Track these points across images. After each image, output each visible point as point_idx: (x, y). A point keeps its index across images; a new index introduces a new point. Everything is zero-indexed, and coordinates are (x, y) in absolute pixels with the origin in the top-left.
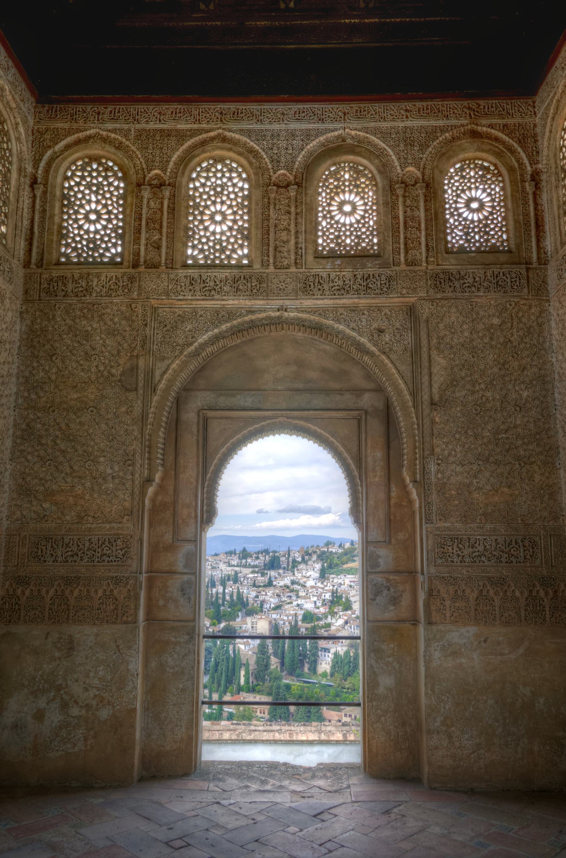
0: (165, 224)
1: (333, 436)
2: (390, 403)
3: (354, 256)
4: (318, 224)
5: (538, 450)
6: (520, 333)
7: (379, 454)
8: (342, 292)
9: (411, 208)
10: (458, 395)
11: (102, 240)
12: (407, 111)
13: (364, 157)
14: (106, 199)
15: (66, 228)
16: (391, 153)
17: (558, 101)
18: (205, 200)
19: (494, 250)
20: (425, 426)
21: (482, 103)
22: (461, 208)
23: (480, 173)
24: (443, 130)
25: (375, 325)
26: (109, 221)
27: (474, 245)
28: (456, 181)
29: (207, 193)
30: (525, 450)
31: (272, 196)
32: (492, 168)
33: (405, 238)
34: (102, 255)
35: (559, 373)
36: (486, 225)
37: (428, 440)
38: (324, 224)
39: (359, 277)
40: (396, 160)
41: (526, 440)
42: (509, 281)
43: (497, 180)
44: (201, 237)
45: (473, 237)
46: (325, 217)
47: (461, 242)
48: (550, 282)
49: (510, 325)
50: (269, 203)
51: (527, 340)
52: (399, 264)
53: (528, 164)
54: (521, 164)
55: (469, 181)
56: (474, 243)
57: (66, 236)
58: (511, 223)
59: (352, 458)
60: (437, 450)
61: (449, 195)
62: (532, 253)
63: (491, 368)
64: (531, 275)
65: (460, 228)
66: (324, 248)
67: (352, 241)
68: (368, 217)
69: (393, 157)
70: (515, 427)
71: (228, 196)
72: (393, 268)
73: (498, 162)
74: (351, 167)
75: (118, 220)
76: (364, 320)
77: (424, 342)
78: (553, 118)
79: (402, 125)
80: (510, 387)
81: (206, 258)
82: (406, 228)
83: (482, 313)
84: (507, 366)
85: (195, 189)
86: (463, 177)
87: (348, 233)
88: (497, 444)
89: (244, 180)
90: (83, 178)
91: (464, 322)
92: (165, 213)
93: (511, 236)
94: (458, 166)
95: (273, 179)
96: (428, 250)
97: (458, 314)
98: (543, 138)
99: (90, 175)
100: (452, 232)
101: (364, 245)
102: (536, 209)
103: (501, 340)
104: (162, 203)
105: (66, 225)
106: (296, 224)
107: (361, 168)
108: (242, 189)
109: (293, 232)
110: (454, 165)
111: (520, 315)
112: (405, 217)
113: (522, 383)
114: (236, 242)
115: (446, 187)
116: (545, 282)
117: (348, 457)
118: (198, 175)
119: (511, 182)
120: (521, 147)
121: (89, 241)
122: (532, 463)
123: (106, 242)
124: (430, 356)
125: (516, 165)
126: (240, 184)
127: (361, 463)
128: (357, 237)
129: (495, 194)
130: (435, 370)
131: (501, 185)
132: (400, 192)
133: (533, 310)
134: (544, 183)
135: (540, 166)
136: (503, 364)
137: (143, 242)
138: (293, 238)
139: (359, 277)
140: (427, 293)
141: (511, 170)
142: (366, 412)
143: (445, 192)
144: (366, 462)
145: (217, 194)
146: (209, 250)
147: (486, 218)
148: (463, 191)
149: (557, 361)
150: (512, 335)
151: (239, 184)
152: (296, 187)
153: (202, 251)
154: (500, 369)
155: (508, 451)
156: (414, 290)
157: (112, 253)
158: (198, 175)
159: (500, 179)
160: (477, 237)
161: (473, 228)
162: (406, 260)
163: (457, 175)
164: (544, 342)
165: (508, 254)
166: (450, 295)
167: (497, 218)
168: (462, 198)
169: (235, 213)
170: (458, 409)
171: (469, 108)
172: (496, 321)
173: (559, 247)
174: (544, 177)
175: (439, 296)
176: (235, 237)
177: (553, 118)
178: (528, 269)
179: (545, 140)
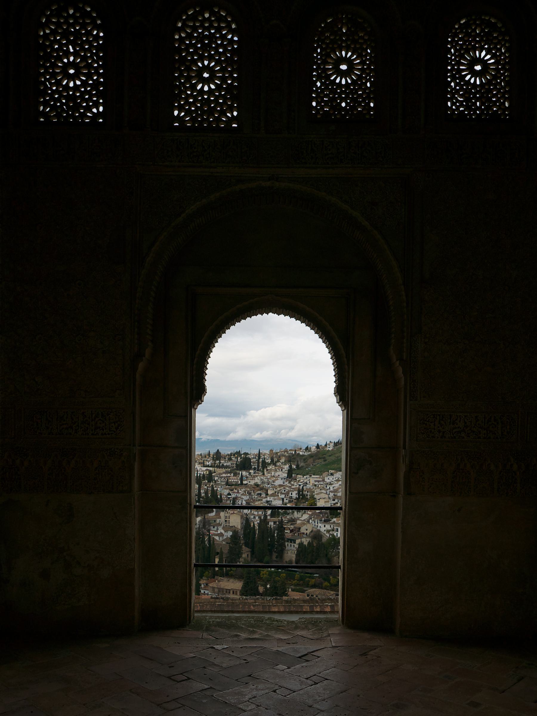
11: (82, 97)
14: (85, 50)
15: (44, 83)
18: (192, 54)
22: (463, 70)
26: (89, 76)
28: (460, 39)
29: (194, 46)
32: (499, 25)
34: (83, 115)
38: (319, 84)
43: (503, 39)
44: (188, 97)
46: (319, 78)
57: (44, 93)
61: (452, 55)
66: (318, 111)
68: (366, 77)
71: (216, 49)
75: (99, 75)
81: (193, 120)
86: (468, 35)
90: (58, 25)
99: (66, 22)
105: (43, 79)
114: (225, 102)
121: (68, 98)
123: (87, 101)
129: (500, 56)
145: (205, 47)
146: (196, 111)
153: (188, 112)
157: (93, 113)
163: (461, 32)
167: (500, 83)
168: (465, 59)
169: (222, 70)
176: (224, 97)
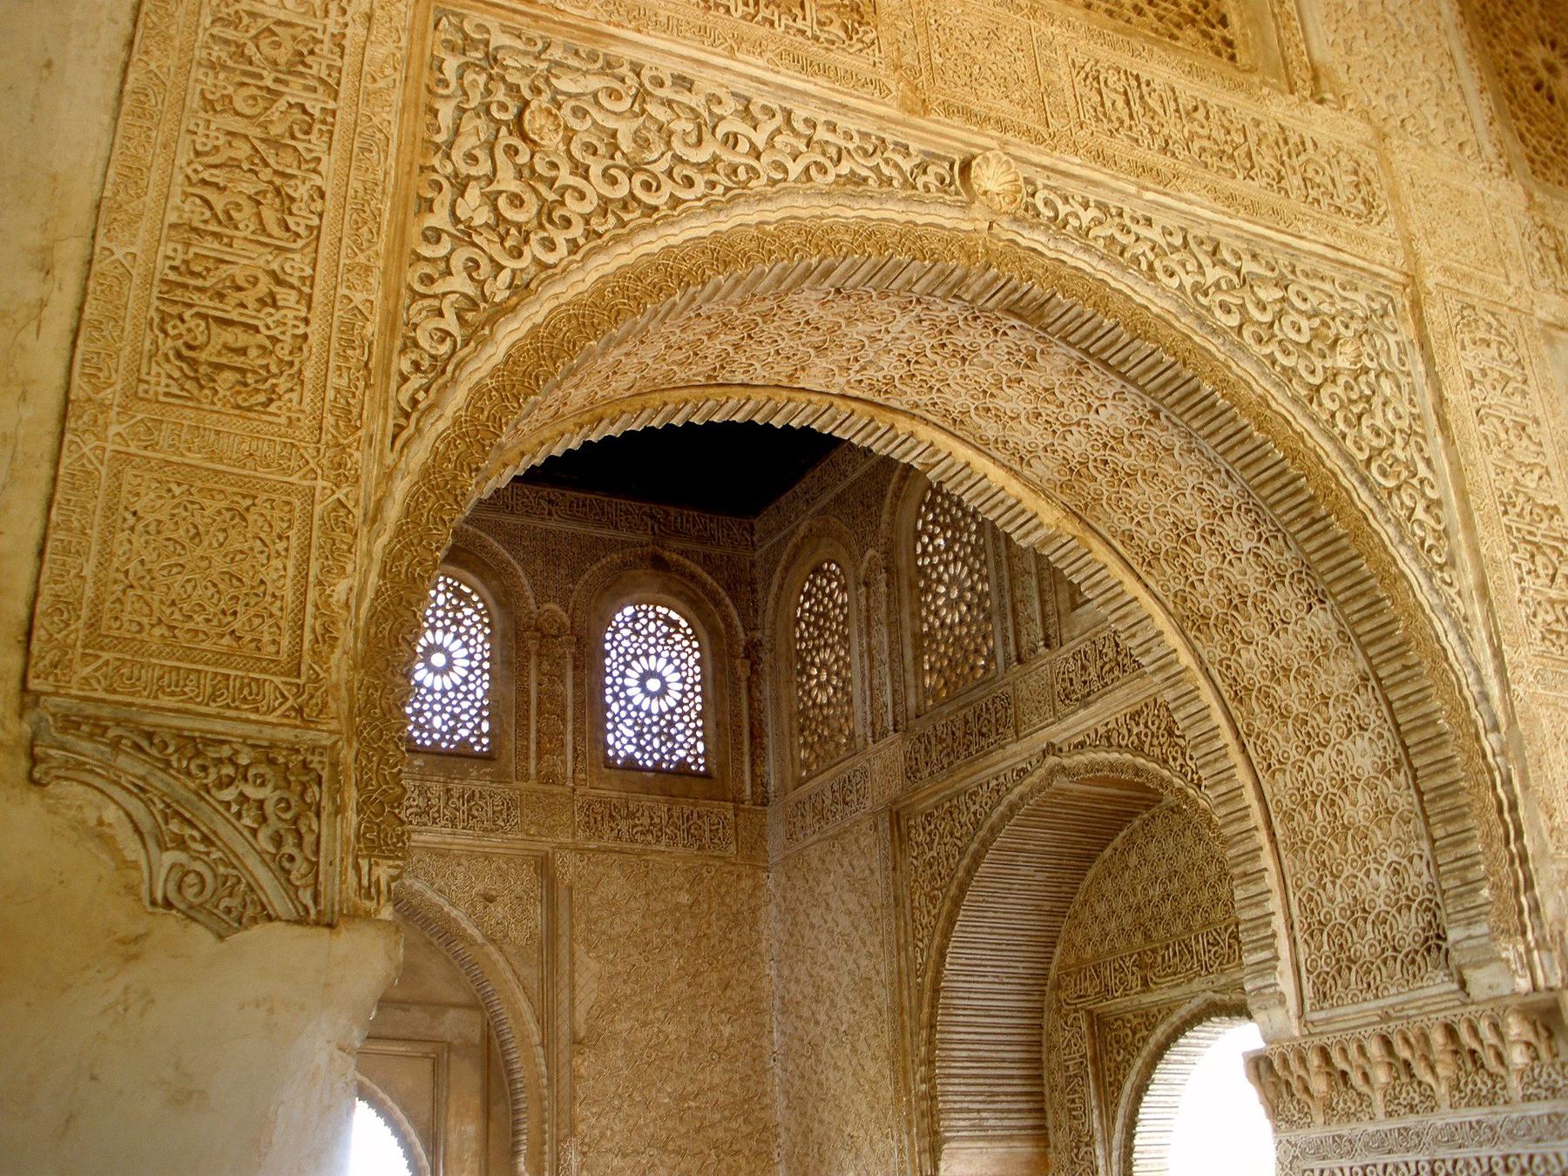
1: (385, 1090)
2: (493, 1032)
3: (448, 754)
5: (745, 1129)
6: (722, 923)
7: (471, 1128)
8: (425, 819)
9: (550, 674)
10: (618, 1027)
12: (550, 502)
13: (473, 572)
16: (521, 573)
17: (797, 546)
19: (682, 769)
20: (562, 1083)
21: (672, 511)
23: (665, 629)
24: (610, 546)
25: (479, 888)
27: (651, 757)
30: (726, 1130)
33: (538, 731)
35: (782, 998)
36: (671, 724)
37: (567, 1107)
39: (456, 794)
40: (527, 587)
41: (727, 1113)
42: (707, 828)
45: (650, 743)
47: (630, 749)
48: (770, 838)
49: (706, 906)
51: (733, 935)
52: (526, 778)
53: (740, 629)
54: (729, 626)
55: (646, 641)
56: (651, 754)
58: (712, 725)
59: (421, 1134)
60: (582, 1127)
62: (743, 782)
63: (675, 981)
64: (741, 822)
65: (629, 722)
67: (444, 723)
69: (524, 580)
70: (711, 1088)
72: (515, 784)
73: (692, 615)
74: (448, 586)
76: (461, 876)
77: (564, 927)
78: (786, 569)
79: (541, 525)
80: (705, 1017)
82: (540, 712)
83: (663, 883)
84: (699, 980)
86: (637, 633)
87: (437, 707)
88: (681, 1119)
91: (632, 895)
93: (711, 747)
94: (629, 611)
96: (575, 758)
97: (622, 881)
98: (767, 594)
100: (615, 729)
101: (464, 733)
102: (750, 707)
103: (693, 934)
107: (467, 590)
110: (620, 610)
111: (723, 890)
112: (539, 693)
113: (722, 1011)
115: (608, 646)
116: (762, 836)
117: (412, 1131)
119: (713, 654)
120: (731, 598)
122: (737, 1152)
124: (572, 954)
125: (722, 626)
127: (436, 1146)
128: (454, 716)
130: (579, 981)
131: (697, 655)
132: (533, 645)
133: (743, 884)
134: (765, 667)
135: (758, 635)
136: (694, 976)
139: (456, 794)
140: (574, 835)
141: (713, 633)
142: (450, 1046)
143: (607, 654)
144: (446, 1141)
147: (672, 711)
148: (636, 657)
149: (780, 976)
150: (709, 925)
154: (689, 985)
155: (698, 1131)
156: (552, 829)
159: (695, 645)
160: (656, 743)
161: (650, 726)
162: (538, 772)
163: (626, 627)
164: (759, 941)
165: (706, 781)
166: (611, 845)
167: (688, 713)
170: (619, 1053)
171: (652, 517)
172: (685, 898)
173: (789, 783)
174: (766, 657)
175: (593, 845)
177: (786, 569)
178: (736, 809)
179: (772, 596)
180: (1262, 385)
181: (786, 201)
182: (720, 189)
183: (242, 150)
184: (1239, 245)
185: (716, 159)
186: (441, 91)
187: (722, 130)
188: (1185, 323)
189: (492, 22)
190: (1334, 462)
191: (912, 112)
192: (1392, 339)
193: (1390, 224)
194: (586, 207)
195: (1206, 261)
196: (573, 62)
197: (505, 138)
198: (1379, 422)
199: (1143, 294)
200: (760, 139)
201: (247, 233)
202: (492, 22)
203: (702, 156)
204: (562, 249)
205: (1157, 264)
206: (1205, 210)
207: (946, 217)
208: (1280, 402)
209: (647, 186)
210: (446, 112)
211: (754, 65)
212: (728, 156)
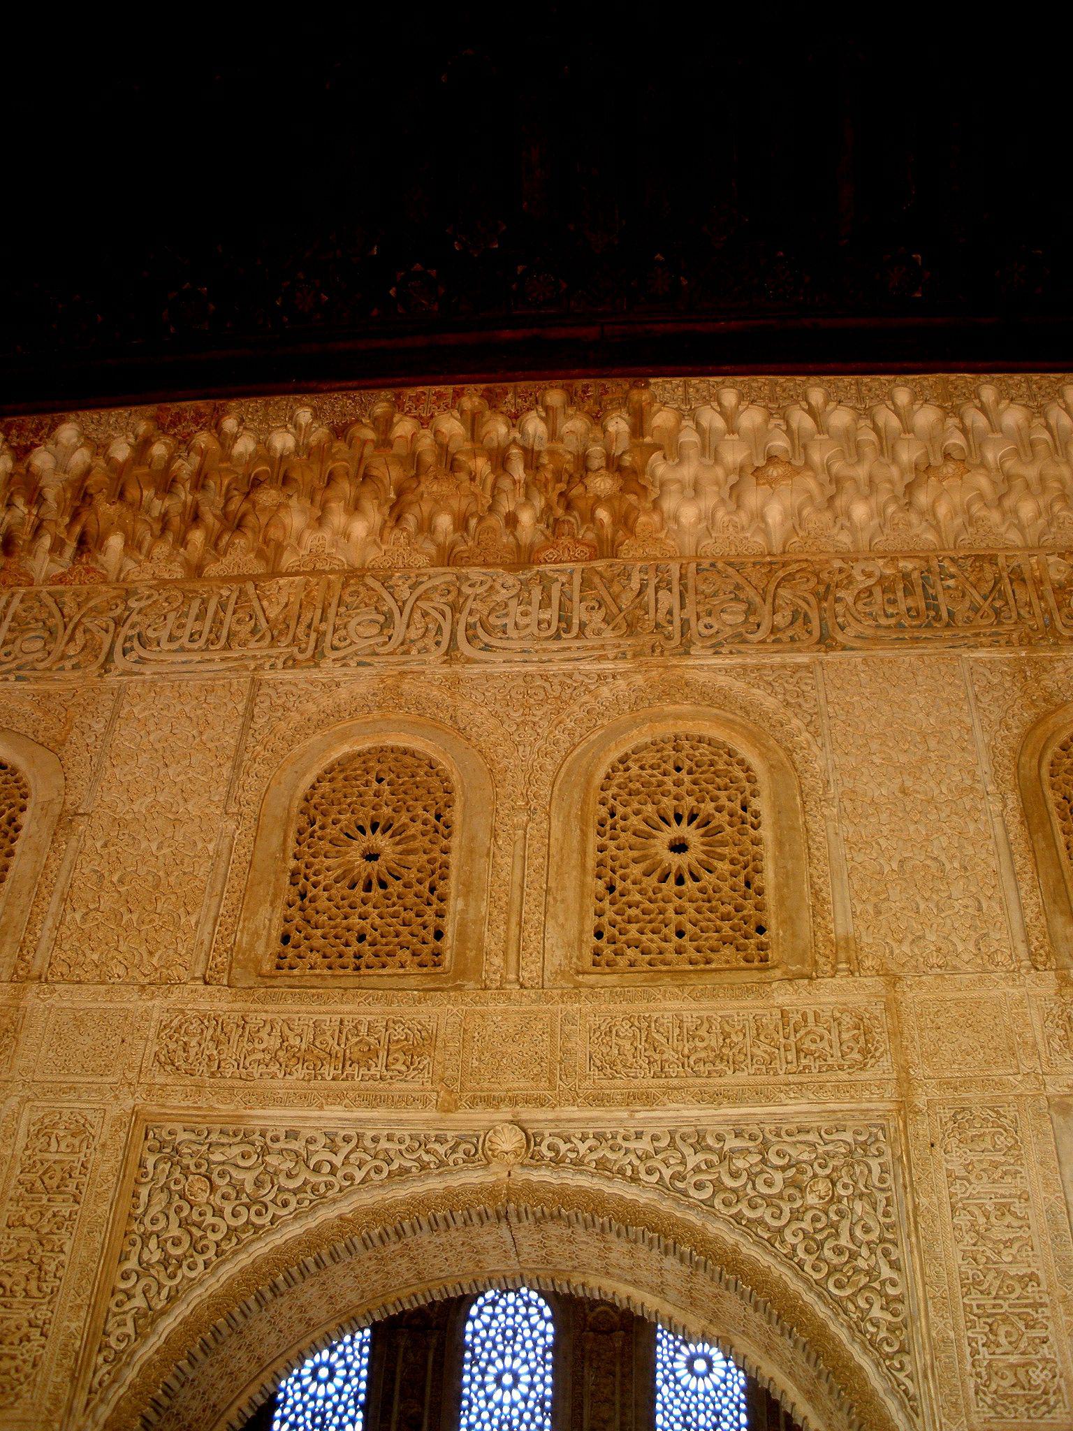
0: (428, 1390)
4: (656, 1390)
31: (588, 1347)
38: (665, 1389)
50: (583, 1357)
85: (475, 1333)
89: (547, 1321)
92: (429, 1373)
95: (590, 1319)
104: (425, 1357)
106: (623, 1392)
108: (543, 1334)
109: (618, 1406)
118: (481, 1311)
126: (541, 1325)
137: (395, 1417)
138: (618, 1416)
151: (541, 1327)
152: (622, 1333)
158: (481, 1311)
180: (731, 1237)
181: (355, 1197)
182: (307, 1203)
183: (25, 1247)
184: (720, 1129)
185: (305, 1183)
186: (143, 1180)
187: (312, 1164)
188: (666, 1206)
189: (178, 1127)
190: (795, 1285)
191: (449, 1111)
192: (874, 1164)
193: (886, 1063)
194: (219, 1236)
195: (688, 1151)
196: (224, 1140)
197: (177, 1201)
198: (844, 1241)
199: (630, 1192)
200: (337, 1161)
201: (20, 1299)
202: (178, 1127)
203: (297, 1183)
204: (201, 1267)
205: (642, 1169)
206: (691, 1113)
207: (474, 1177)
208: (749, 1250)
209: (259, 1214)
210: (144, 1192)
211: (334, 1113)
212: (314, 1179)
